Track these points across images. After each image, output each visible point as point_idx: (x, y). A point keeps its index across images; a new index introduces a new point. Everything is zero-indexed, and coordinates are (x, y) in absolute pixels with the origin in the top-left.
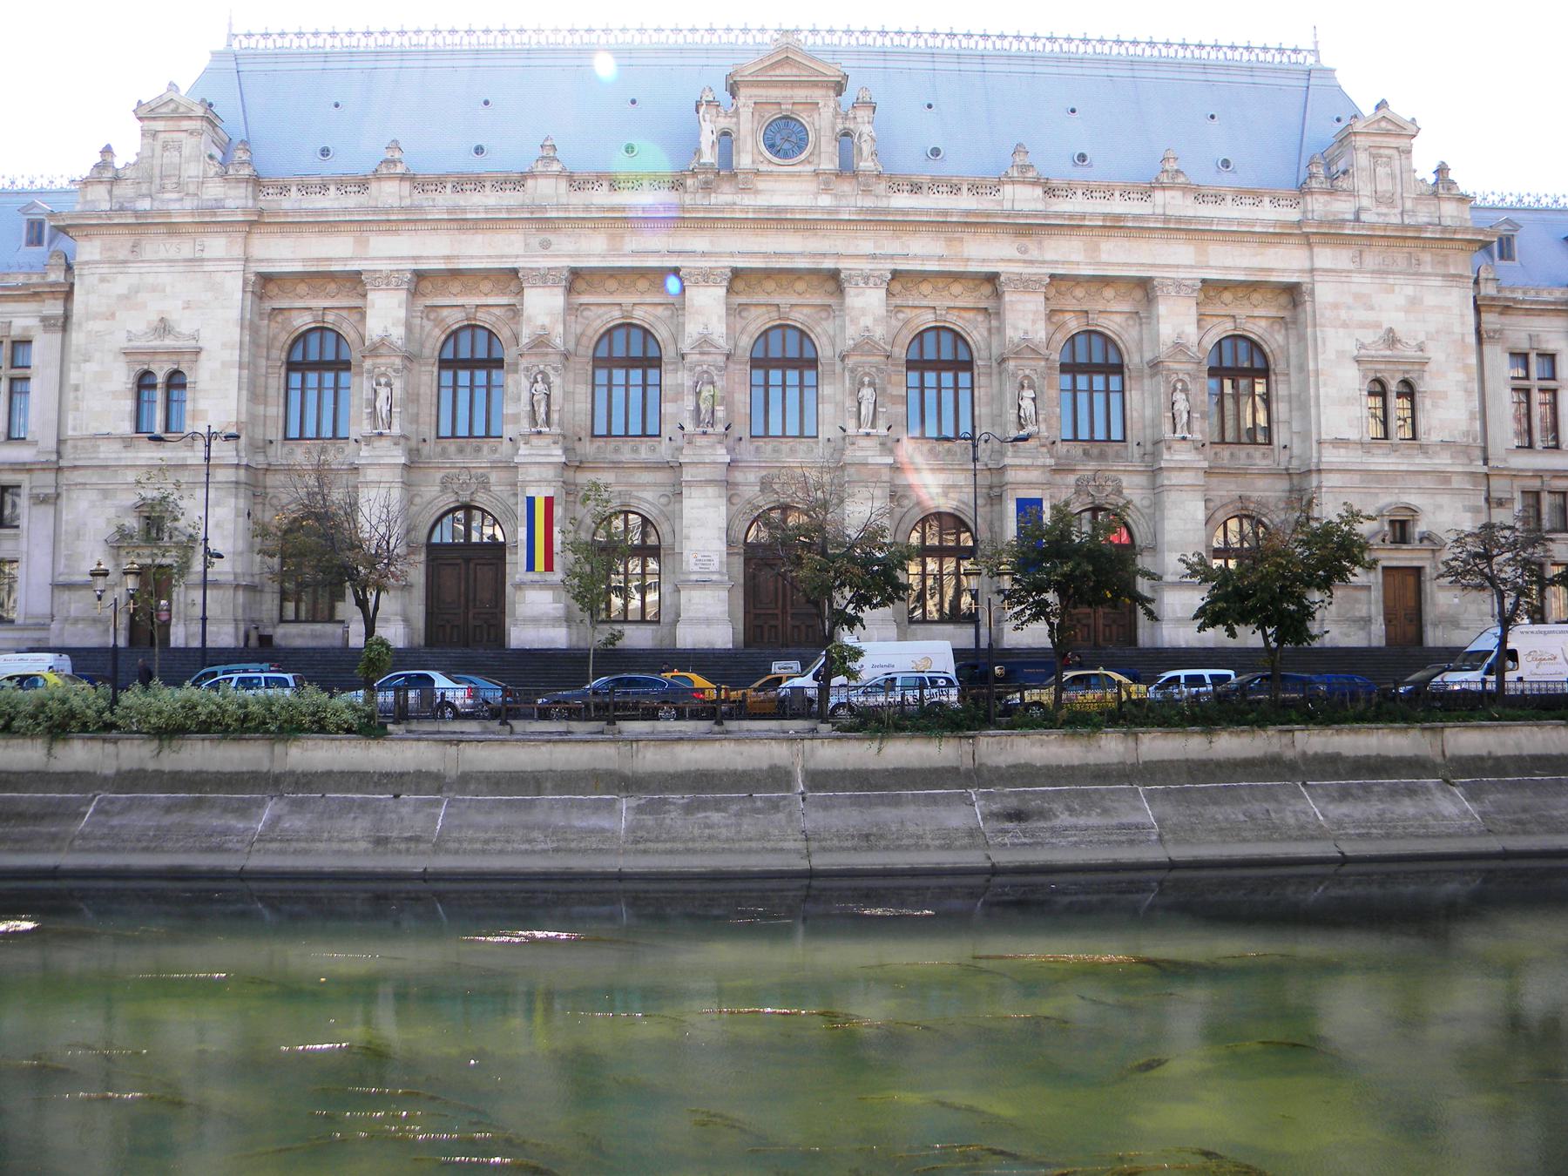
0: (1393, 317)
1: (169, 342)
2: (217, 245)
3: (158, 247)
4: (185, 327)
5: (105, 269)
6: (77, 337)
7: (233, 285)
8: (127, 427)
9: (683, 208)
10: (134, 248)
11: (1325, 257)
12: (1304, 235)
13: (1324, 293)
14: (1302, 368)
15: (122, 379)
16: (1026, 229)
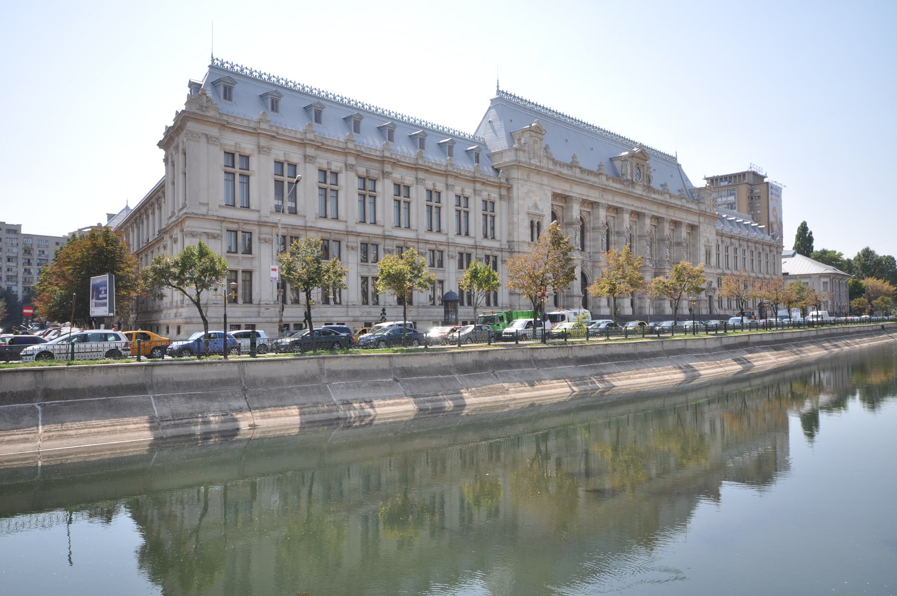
0: (708, 235)
1: (537, 212)
2: (545, 180)
3: (534, 178)
4: (540, 207)
5: (522, 182)
6: (515, 205)
7: (550, 195)
8: (529, 240)
9: (561, 173)
10: (528, 176)
11: (702, 219)
12: (701, 214)
13: (702, 228)
14: (694, 246)
15: (527, 223)
16: (668, 206)
